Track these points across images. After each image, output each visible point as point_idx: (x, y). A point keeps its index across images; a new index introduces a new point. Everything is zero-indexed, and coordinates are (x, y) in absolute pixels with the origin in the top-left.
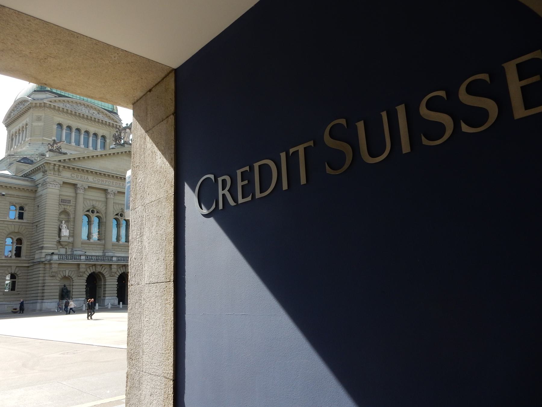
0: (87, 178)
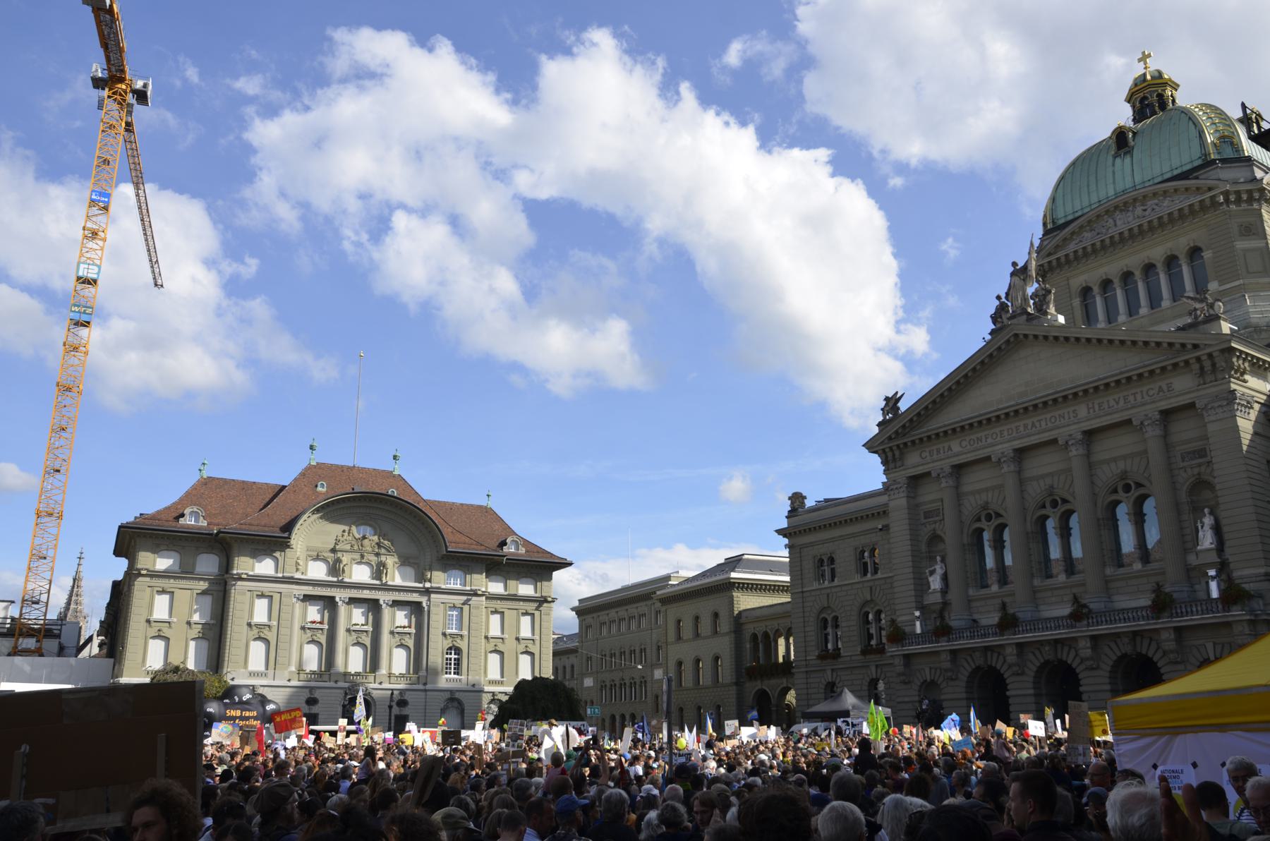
0: (950, 449)
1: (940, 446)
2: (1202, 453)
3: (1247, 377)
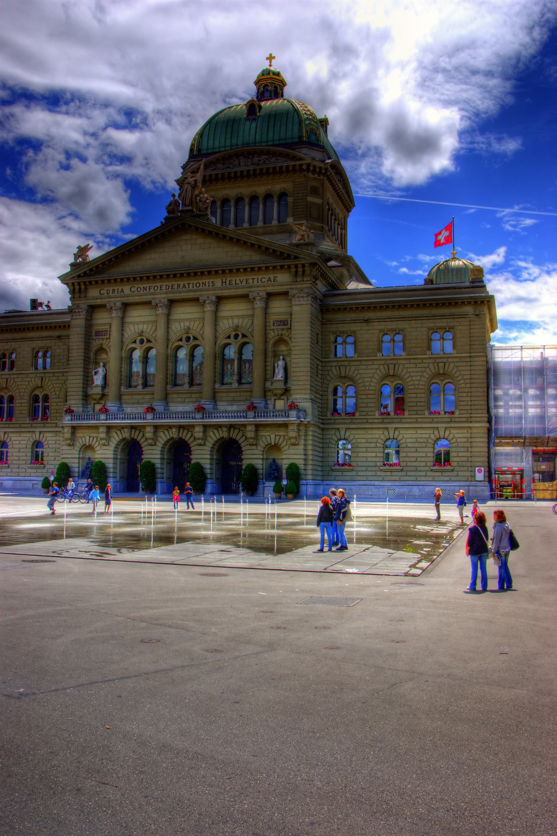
0: (122, 291)
1: (116, 288)
2: (284, 323)
3: (318, 282)
